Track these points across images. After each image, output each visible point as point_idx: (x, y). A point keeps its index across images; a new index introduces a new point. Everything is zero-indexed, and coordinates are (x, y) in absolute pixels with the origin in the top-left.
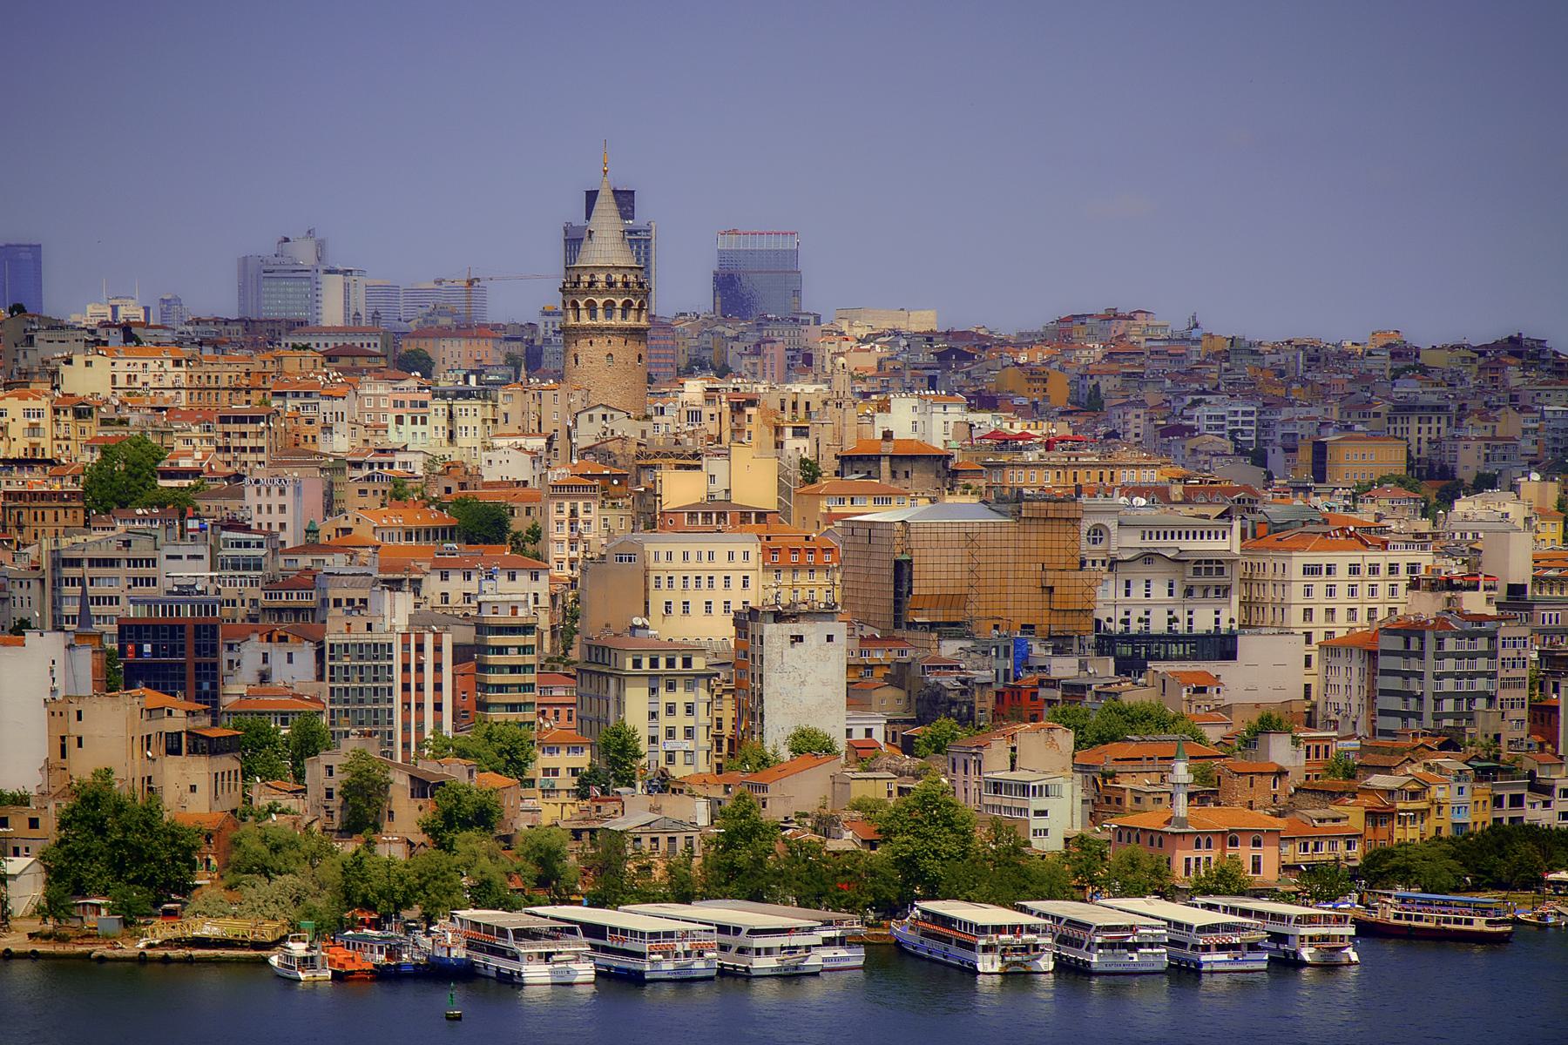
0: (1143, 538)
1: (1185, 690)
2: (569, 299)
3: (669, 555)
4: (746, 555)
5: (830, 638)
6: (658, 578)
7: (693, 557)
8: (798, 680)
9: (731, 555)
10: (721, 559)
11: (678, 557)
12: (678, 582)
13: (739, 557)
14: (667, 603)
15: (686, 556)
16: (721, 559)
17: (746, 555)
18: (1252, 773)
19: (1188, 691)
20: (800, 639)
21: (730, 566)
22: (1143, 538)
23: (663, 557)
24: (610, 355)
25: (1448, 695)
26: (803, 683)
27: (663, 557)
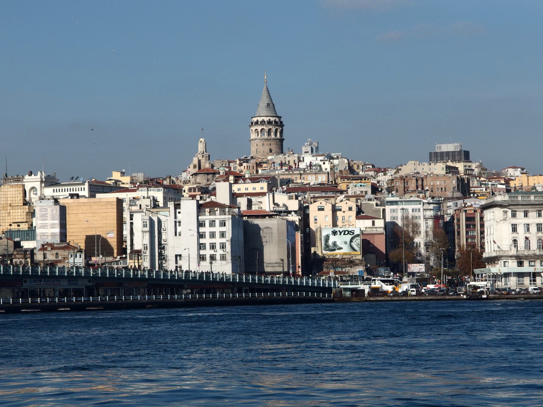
0: (54, 192)
22: (54, 192)
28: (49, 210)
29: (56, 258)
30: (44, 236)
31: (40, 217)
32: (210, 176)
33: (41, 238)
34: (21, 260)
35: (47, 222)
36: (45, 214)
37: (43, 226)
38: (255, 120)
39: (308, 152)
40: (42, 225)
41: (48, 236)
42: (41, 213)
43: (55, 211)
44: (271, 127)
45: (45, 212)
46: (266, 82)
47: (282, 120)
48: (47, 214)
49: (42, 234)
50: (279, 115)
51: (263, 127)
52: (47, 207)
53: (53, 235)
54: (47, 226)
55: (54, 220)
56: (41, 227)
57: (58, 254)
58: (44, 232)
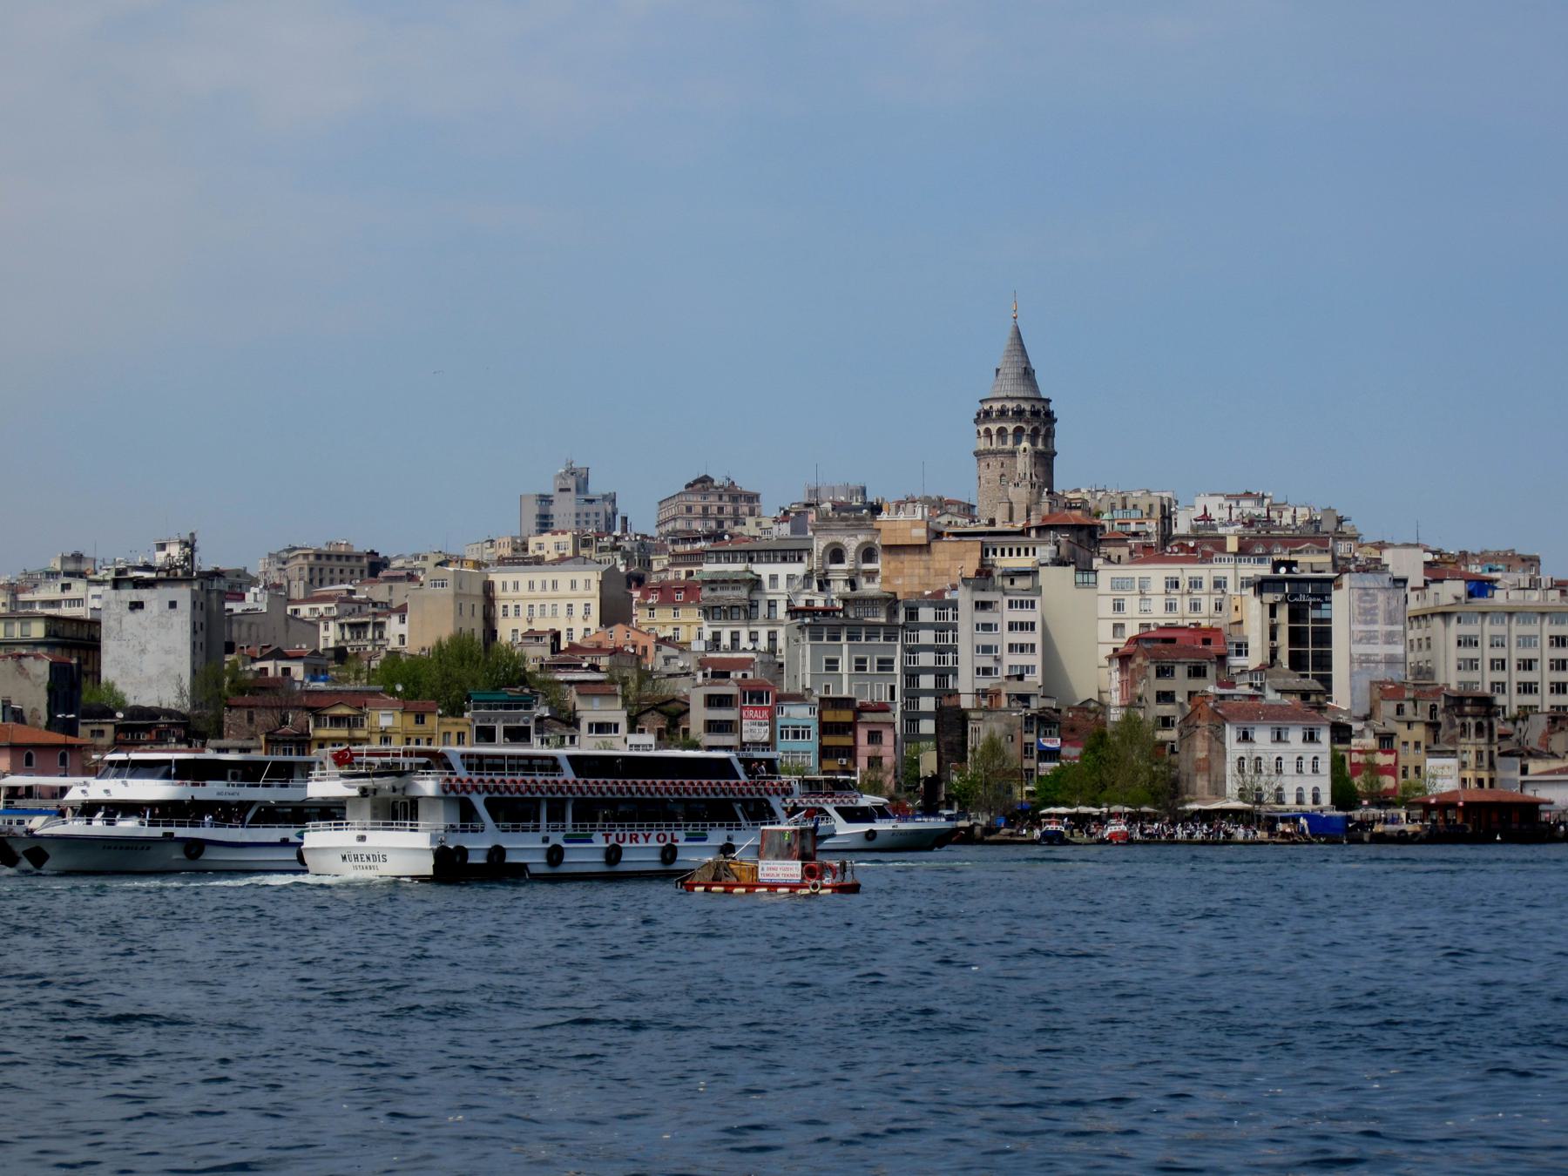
1: (700, 674)
2: (982, 428)
3: (516, 585)
4: (588, 582)
5: (173, 605)
6: (505, 607)
7: (538, 586)
8: (138, 648)
9: (573, 584)
10: (564, 587)
11: (524, 586)
12: (524, 612)
13: (580, 585)
14: (513, 631)
15: (531, 585)
16: (564, 587)
17: (588, 582)
18: (250, 707)
19: (705, 675)
20: (137, 606)
21: (574, 593)
23: (510, 586)
24: (1002, 475)
25: (926, 670)
26: (143, 651)
27: (510, 586)
28: (1381, 597)
29: (1431, 718)
30: (1368, 661)
31: (1360, 614)
32: (1084, 535)
33: (1361, 667)
34: (1479, 720)
35: (1376, 627)
36: (1372, 609)
37: (1366, 638)
38: (987, 407)
39: (569, 490)
40: (1364, 634)
41: (1377, 662)
42: (1362, 605)
43: (1394, 603)
44: (1037, 424)
45: (1371, 602)
46: (1015, 318)
47: (1052, 407)
48: (1376, 607)
49: (1363, 658)
50: (1044, 396)
51: (1018, 424)
52: (1376, 591)
53: (1391, 661)
54: (1376, 638)
55: (1392, 624)
56: (1361, 640)
57: (1436, 709)
58: (1369, 652)
